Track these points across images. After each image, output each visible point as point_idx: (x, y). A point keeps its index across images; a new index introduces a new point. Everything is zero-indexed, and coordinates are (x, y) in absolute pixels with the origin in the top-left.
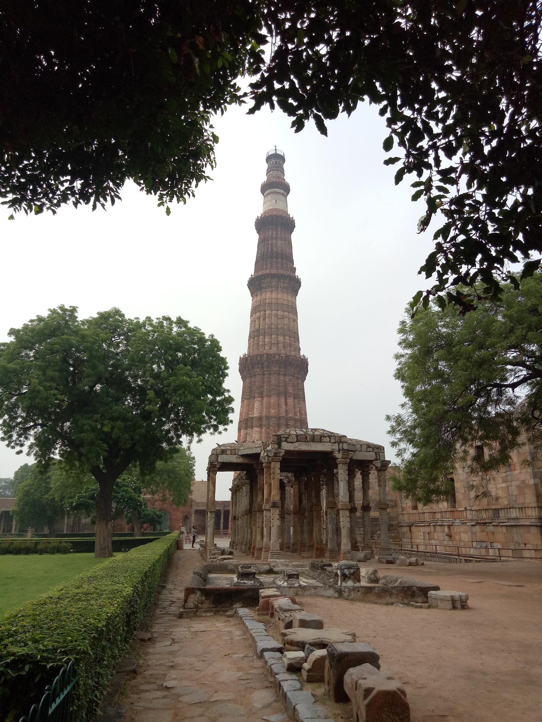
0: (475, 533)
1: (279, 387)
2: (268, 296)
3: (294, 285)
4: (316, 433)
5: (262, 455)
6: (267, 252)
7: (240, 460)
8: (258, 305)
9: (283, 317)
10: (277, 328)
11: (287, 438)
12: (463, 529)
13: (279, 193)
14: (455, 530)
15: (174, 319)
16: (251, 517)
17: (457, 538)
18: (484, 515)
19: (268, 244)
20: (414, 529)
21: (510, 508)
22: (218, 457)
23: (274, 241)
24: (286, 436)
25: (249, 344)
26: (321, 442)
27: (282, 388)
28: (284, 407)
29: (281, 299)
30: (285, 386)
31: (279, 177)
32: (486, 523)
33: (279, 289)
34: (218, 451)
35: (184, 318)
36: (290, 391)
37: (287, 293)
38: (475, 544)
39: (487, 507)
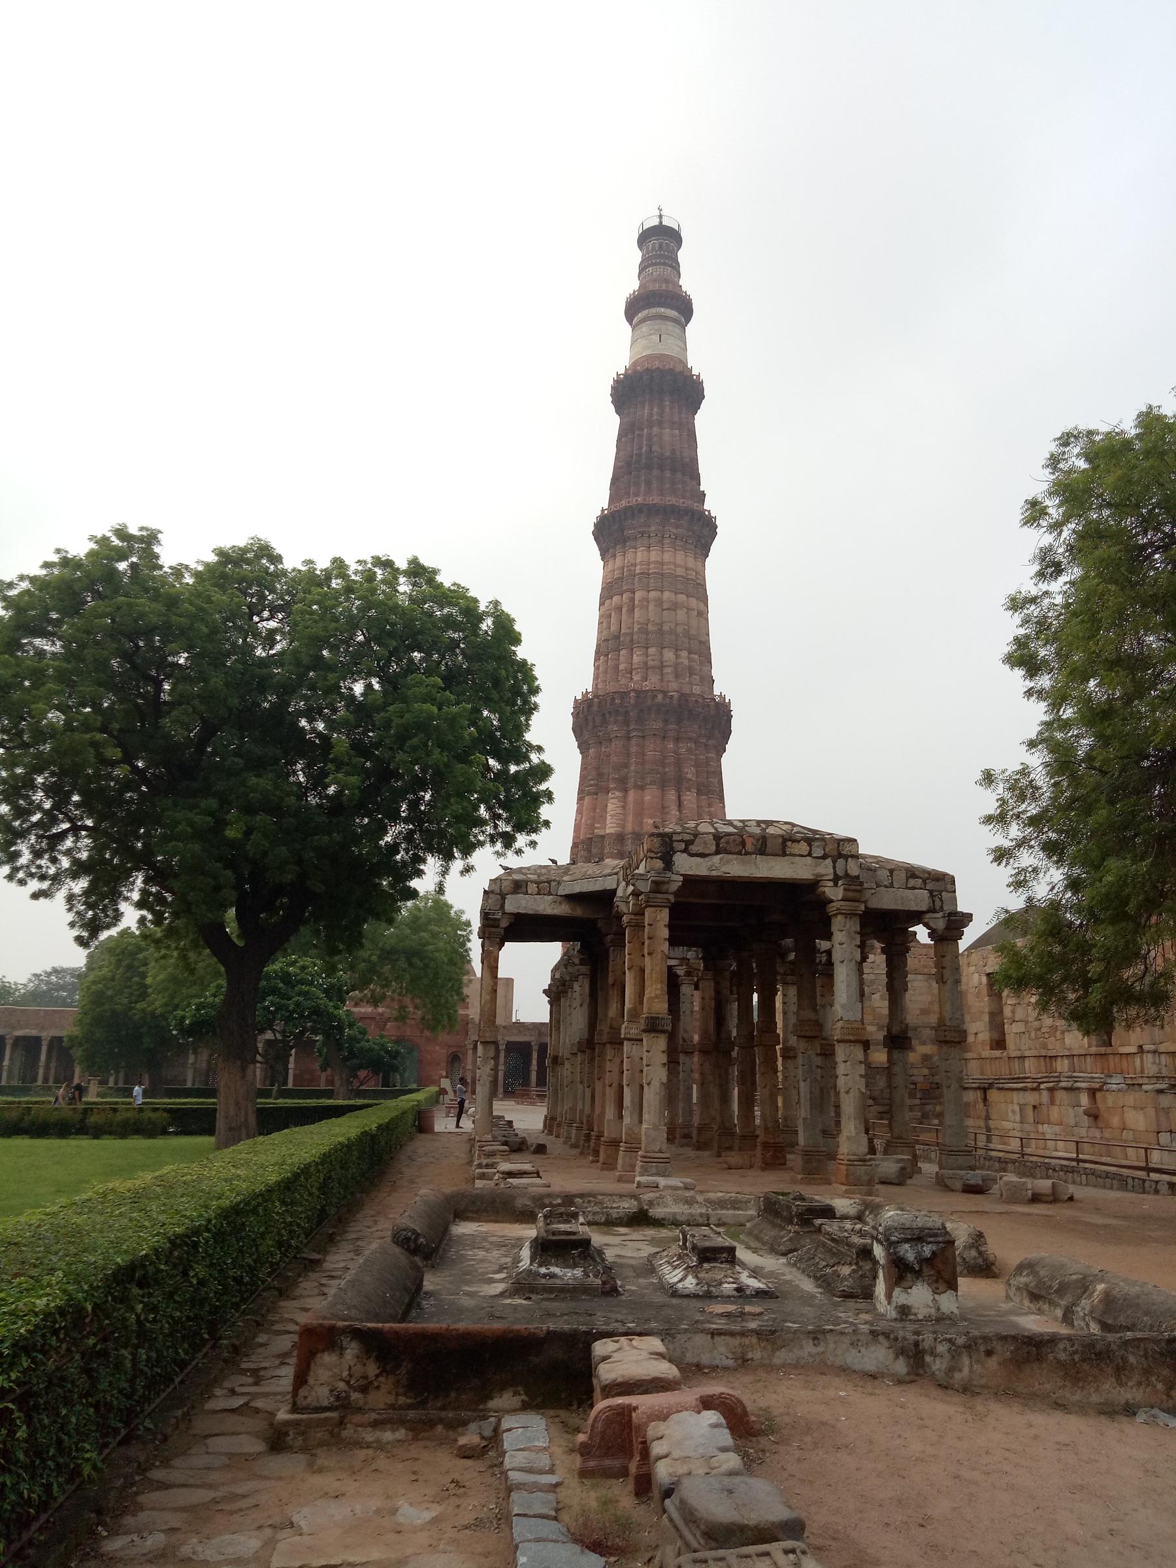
1: (664, 767)
2: (639, 556)
3: (700, 531)
4: (771, 830)
5: (620, 893)
6: (640, 455)
7: (563, 910)
8: (618, 579)
9: (674, 607)
10: (660, 632)
11: (688, 843)
12: (1131, 1098)
14: (1107, 1101)
15: (402, 564)
16: (592, 1060)
17: (1115, 1121)
19: (640, 436)
20: (993, 1095)
24: (687, 837)
25: (597, 668)
26: (784, 854)
27: (670, 770)
28: (674, 812)
29: (670, 563)
30: (679, 764)
31: (667, 281)
33: (667, 541)
34: (505, 884)
35: (427, 561)
36: (689, 776)
37: (685, 550)
38: (1164, 1138)
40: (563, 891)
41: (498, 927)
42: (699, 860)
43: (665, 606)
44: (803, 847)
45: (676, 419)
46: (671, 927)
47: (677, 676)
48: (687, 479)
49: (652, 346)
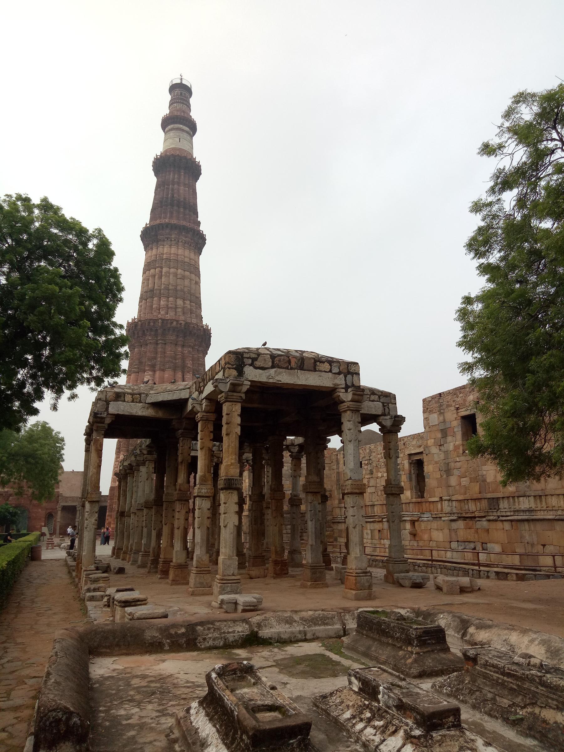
0: (456, 531)
1: (176, 360)
2: (166, 250)
3: (198, 241)
6: (167, 198)
7: (149, 412)
9: (183, 278)
10: (176, 290)
11: (254, 360)
12: (435, 525)
13: (183, 130)
14: (421, 527)
15: (36, 200)
17: (426, 537)
18: (472, 506)
19: (168, 189)
21: (518, 497)
22: (108, 404)
24: (253, 356)
25: (140, 306)
26: (315, 370)
27: (179, 362)
29: (182, 255)
30: (183, 359)
31: (184, 112)
32: (475, 517)
33: (180, 244)
34: (109, 394)
35: (54, 201)
36: (189, 365)
38: (454, 545)
39: (479, 496)
40: (150, 400)
41: (103, 423)
42: (260, 371)
43: (179, 276)
44: (327, 366)
45: (187, 183)
46: (241, 415)
47: (184, 313)
48: (192, 214)
49: (174, 143)
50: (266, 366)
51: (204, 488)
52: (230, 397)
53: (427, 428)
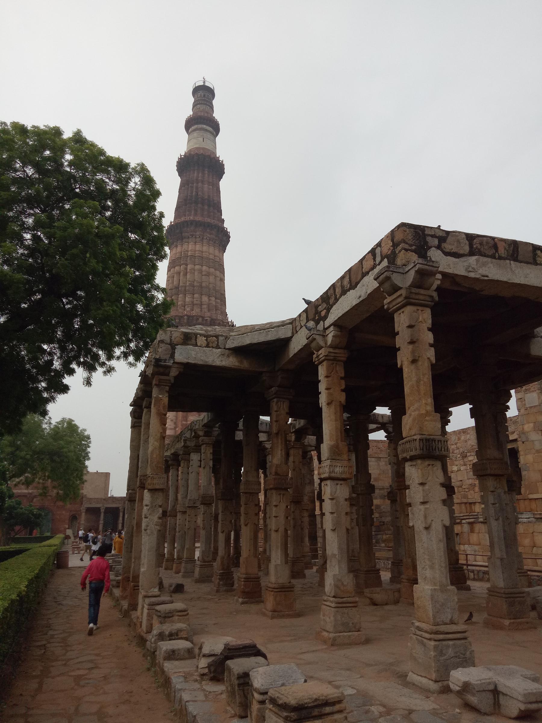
3: (222, 238)
7: (230, 362)
8: (178, 258)
9: (208, 274)
10: (201, 286)
13: (206, 130)
15: (67, 134)
19: (192, 187)
22: (173, 349)
23: (200, 184)
29: (206, 252)
31: (207, 113)
33: (205, 241)
37: (214, 246)
40: (231, 344)
41: (168, 375)
43: (204, 273)
45: (211, 181)
47: (209, 310)
48: (216, 211)
50: (462, 252)
51: (339, 465)
52: (413, 296)
53: (523, 411)
